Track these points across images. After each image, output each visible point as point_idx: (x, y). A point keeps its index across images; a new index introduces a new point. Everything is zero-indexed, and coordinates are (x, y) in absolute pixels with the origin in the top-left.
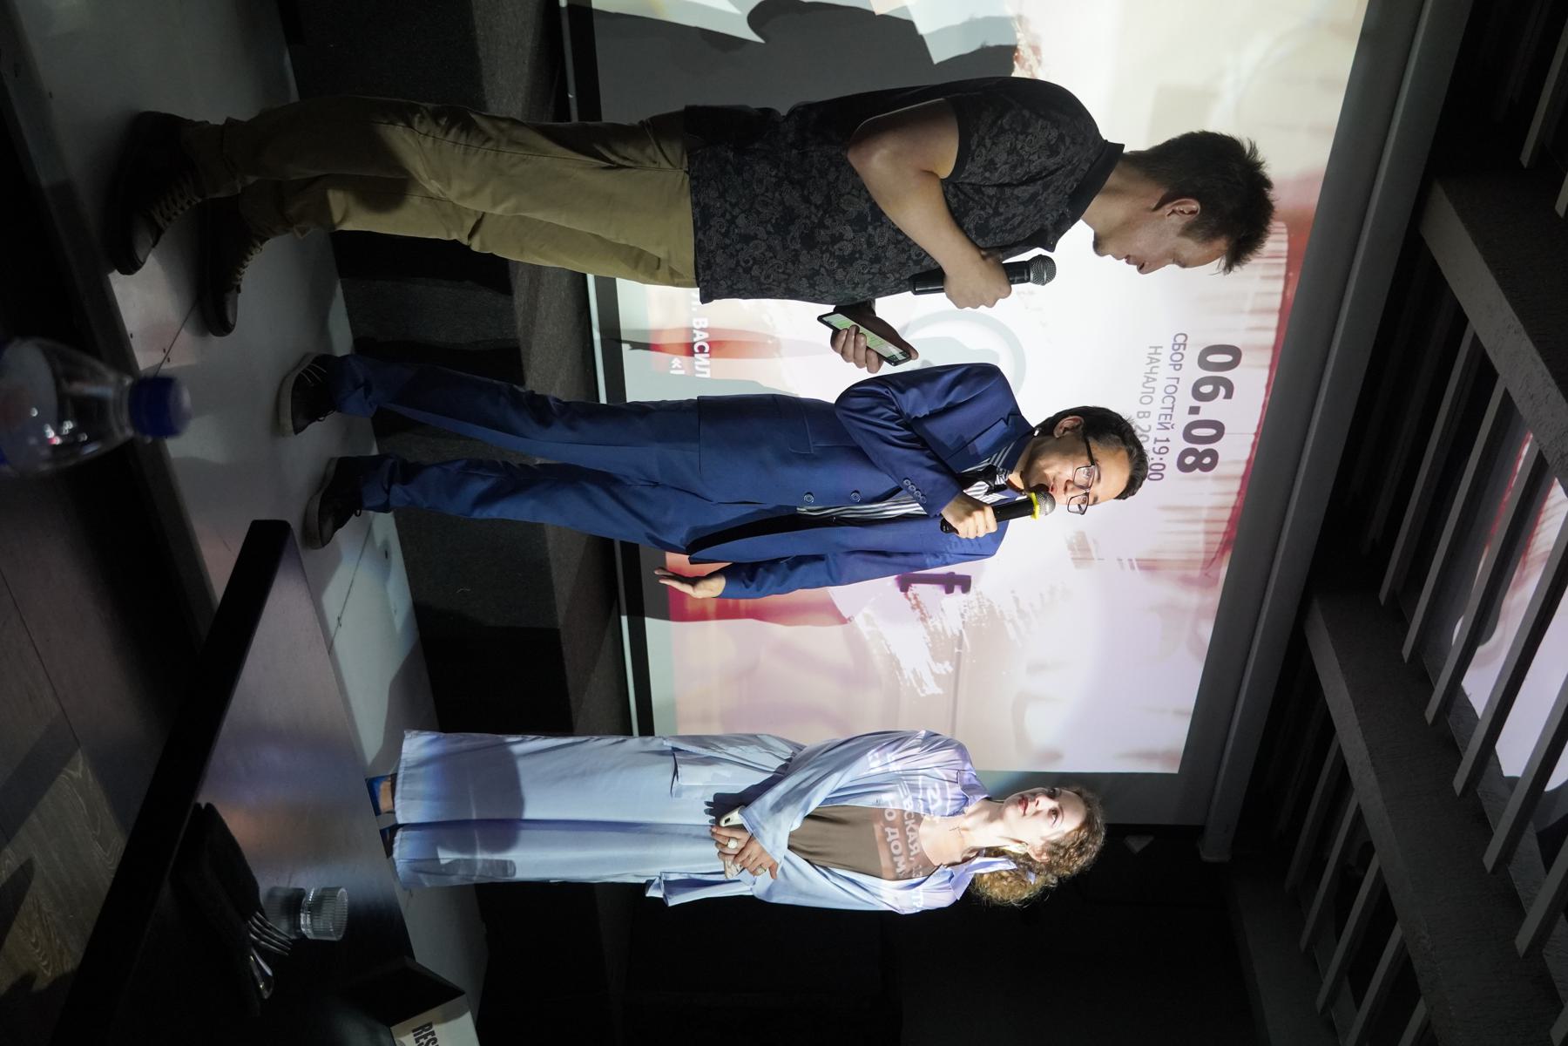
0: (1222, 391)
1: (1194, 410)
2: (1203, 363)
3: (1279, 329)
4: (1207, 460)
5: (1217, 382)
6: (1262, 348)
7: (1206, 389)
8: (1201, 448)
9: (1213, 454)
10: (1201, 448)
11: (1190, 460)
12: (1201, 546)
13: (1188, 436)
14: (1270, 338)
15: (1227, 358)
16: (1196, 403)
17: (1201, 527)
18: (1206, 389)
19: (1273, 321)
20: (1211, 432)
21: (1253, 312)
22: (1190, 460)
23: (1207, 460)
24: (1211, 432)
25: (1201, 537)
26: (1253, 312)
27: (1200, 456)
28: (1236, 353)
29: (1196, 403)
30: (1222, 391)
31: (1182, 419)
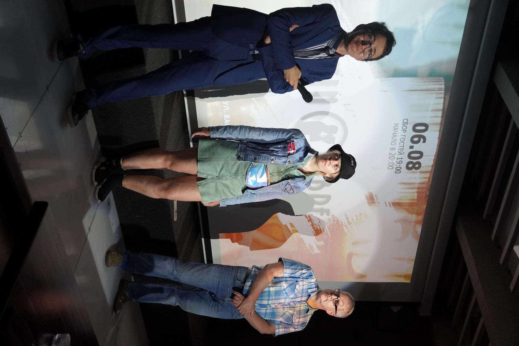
0: (422, 140)
1: (411, 147)
2: (414, 130)
3: (442, 117)
4: (417, 166)
5: (420, 137)
6: (436, 124)
7: (416, 139)
8: (414, 161)
9: (419, 163)
10: (414, 161)
11: (410, 166)
12: (416, 198)
13: (409, 156)
14: (439, 120)
15: (423, 128)
16: (412, 145)
17: (416, 190)
18: (416, 139)
19: (440, 114)
20: (418, 155)
21: (432, 111)
22: (410, 166)
23: (417, 166)
24: (418, 155)
25: (416, 194)
26: (432, 111)
27: (414, 164)
28: (426, 126)
29: (412, 145)
30: (422, 140)
31: (407, 150)
